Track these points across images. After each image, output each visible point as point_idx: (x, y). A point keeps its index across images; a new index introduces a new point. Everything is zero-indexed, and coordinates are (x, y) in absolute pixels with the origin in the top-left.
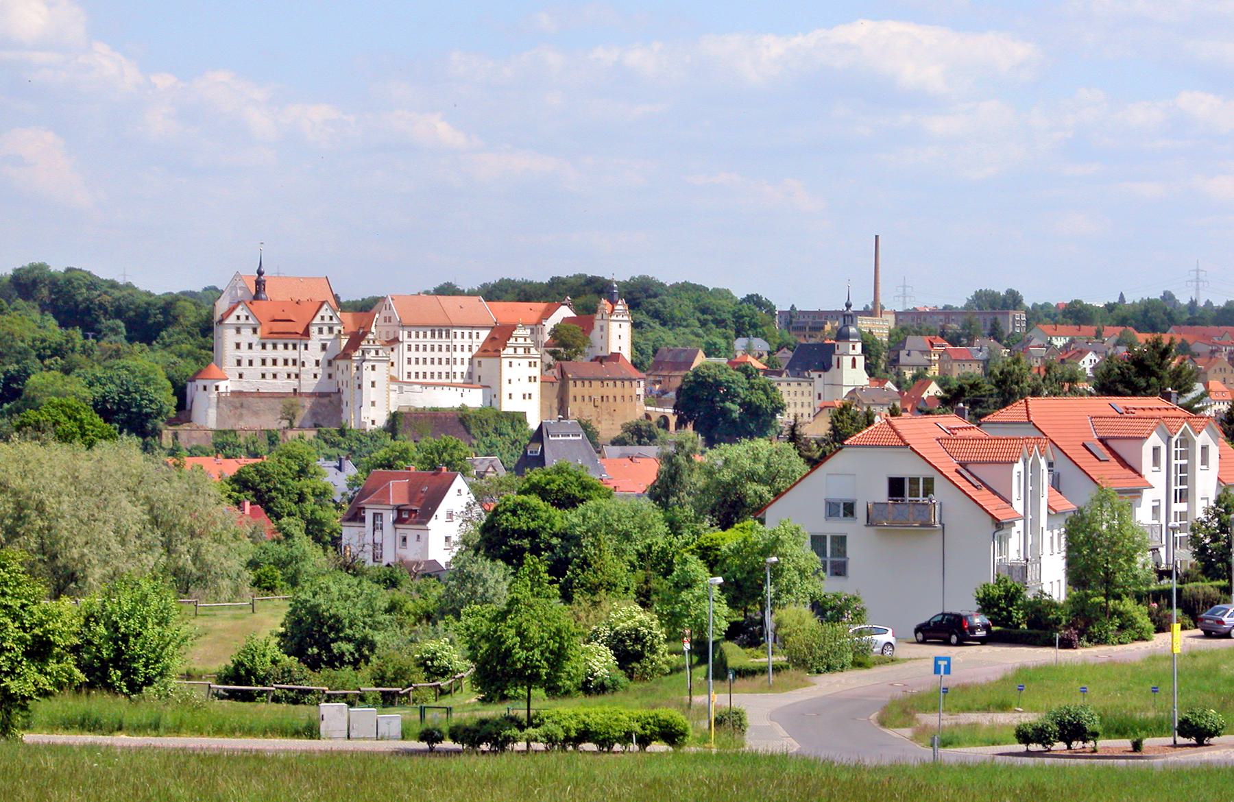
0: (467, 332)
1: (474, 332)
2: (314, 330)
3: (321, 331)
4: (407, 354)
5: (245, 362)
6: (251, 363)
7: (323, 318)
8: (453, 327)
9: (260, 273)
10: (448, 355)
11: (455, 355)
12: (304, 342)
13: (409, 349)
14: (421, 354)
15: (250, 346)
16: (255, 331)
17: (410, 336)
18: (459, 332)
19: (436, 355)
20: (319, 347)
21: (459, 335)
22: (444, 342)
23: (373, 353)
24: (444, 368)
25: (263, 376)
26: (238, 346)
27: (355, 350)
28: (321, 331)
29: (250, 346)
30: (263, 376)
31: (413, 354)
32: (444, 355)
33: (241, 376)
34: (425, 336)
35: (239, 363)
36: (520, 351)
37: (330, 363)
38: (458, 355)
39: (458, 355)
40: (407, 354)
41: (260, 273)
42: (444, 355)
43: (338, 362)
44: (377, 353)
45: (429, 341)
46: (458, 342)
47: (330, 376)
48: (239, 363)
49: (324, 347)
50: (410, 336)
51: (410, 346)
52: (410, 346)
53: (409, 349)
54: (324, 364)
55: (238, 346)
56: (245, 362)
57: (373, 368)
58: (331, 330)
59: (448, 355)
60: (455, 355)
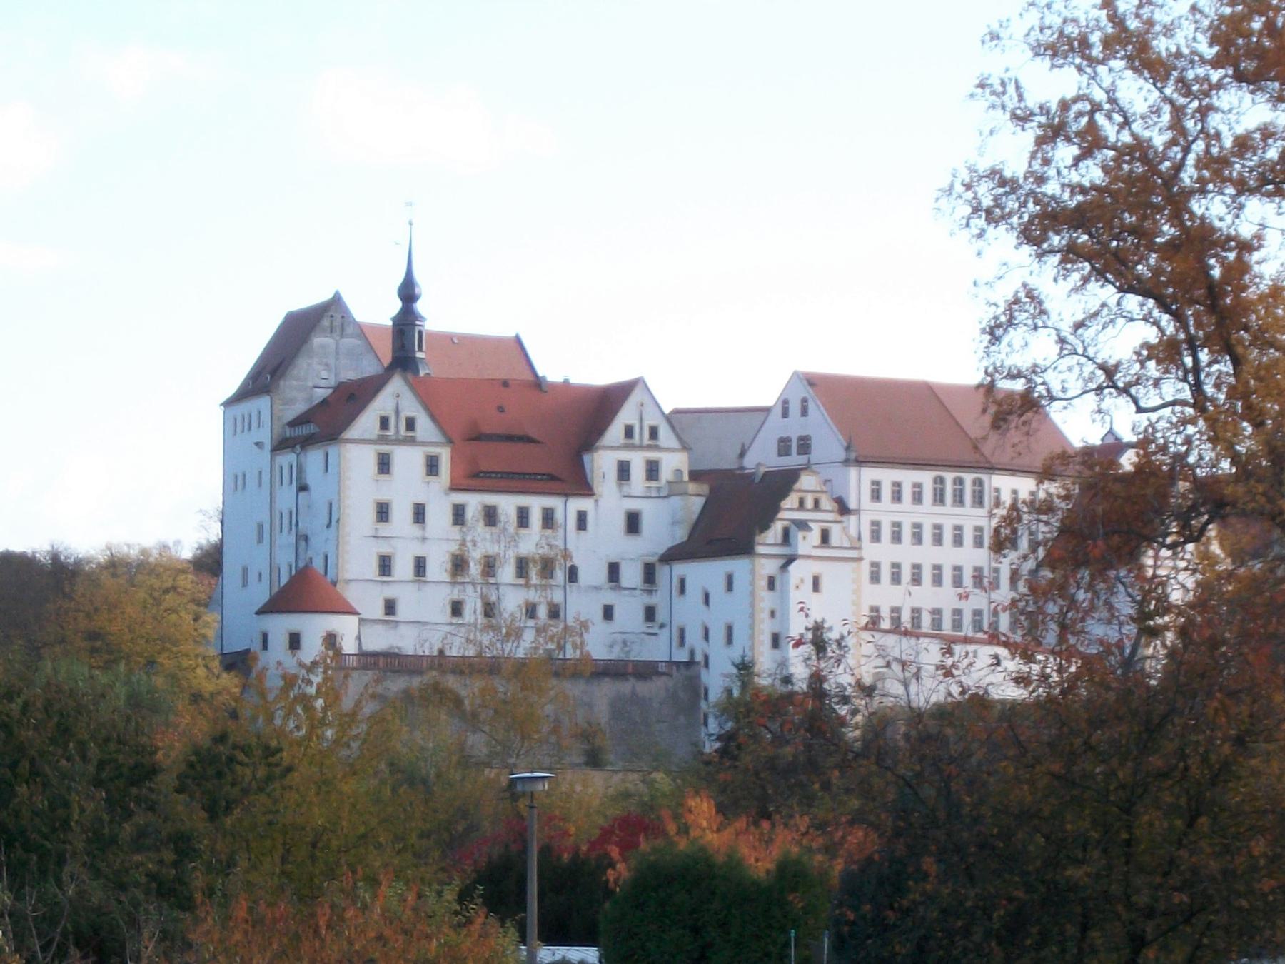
2: (602, 463)
3: (624, 471)
5: (403, 568)
6: (420, 566)
7: (629, 432)
9: (408, 293)
12: (576, 504)
14: (907, 554)
15: (419, 514)
16: (432, 466)
17: (876, 496)
20: (621, 522)
23: (815, 537)
25: (457, 609)
26: (383, 512)
27: (765, 527)
28: (624, 471)
29: (419, 514)
30: (457, 609)
31: (884, 553)
33: (390, 607)
34: (918, 498)
35: (385, 565)
37: (649, 574)
41: (408, 293)
43: (680, 569)
44: (825, 537)
45: (928, 514)
47: (650, 614)
48: (385, 565)
49: (633, 523)
50: (876, 496)
54: (631, 575)
55: (383, 512)
56: (403, 568)
57: (816, 585)
58: (653, 470)
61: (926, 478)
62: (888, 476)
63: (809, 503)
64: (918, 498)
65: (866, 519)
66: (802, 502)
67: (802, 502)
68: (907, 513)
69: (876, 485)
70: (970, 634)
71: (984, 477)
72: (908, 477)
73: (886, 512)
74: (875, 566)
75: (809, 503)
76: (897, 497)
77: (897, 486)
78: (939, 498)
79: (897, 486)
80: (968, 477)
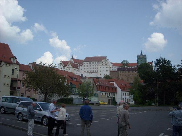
0: (97, 62)
1: (99, 62)
4: (84, 67)
8: (93, 61)
10: (92, 67)
14: (87, 67)
17: (85, 64)
18: (95, 62)
19: (90, 67)
22: (91, 64)
24: (91, 70)
31: (85, 67)
32: (91, 67)
34: (88, 64)
36: (104, 65)
38: (95, 67)
39: (95, 67)
40: (84, 67)
42: (91, 67)
50: (85, 64)
61: (88, 62)
62: (85, 63)
64: (88, 64)
72: (87, 62)
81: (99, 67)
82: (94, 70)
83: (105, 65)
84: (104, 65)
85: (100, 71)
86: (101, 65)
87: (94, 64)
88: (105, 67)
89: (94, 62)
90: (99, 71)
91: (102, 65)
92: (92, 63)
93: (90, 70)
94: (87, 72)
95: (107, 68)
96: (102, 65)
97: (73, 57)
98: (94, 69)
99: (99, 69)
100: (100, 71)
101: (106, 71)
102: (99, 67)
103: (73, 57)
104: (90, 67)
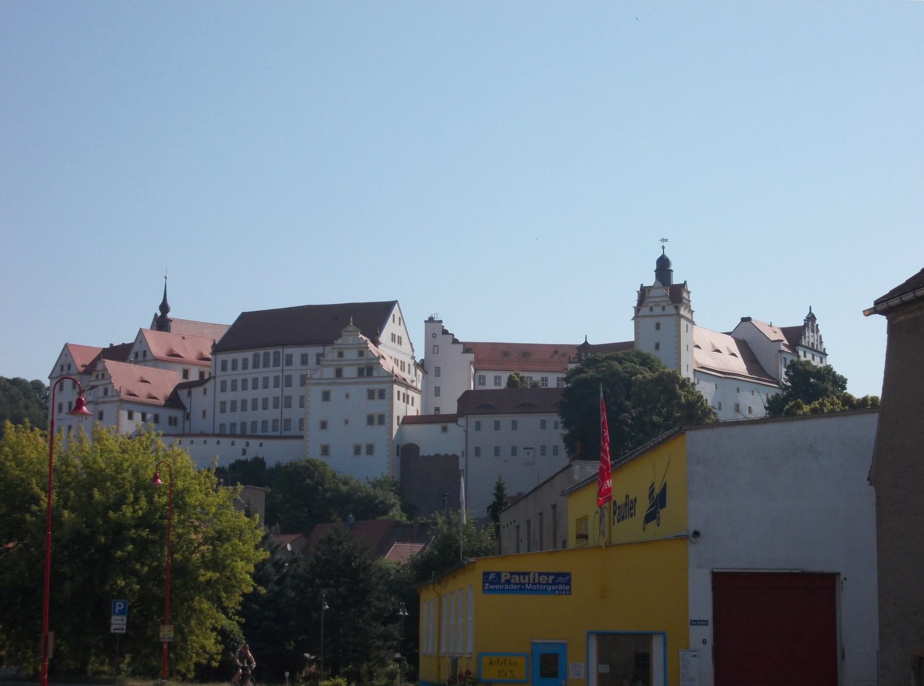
4: (221, 397)
8: (284, 345)
10: (277, 392)
11: (288, 391)
13: (223, 390)
17: (224, 369)
18: (296, 352)
19: (260, 393)
21: (296, 359)
22: (272, 372)
24: (272, 414)
31: (229, 396)
32: (272, 392)
34: (245, 367)
36: (350, 372)
38: (295, 391)
39: (295, 391)
42: (272, 392)
45: (250, 374)
46: (295, 371)
50: (224, 369)
51: (224, 383)
52: (224, 383)
53: (223, 390)
59: (277, 392)
60: (288, 391)
61: (249, 355)
63: (100, 377)
65: (219, 380)
66: (97, 376)
67: (97, 376)
68: (240, 374)
69: (224, 363)
70: (285, 433)
71: (281, 350)
72: (239, 356)
73: (229, 375)
74: (223, 404)
75: (100, 377)
76: (234, 368)
77: (235, 362)
78: (256, 366)
79: (235, 362)
80: (271, 351)
81: (315, 394)
82: (287, 413)
83: (361, 373)
84: (350, 372)
85: (324, 425)
86: (330, 373)
87: (288, 370)
88: (364, 389)
89: (288, 351)
90: (313, 424)
91: (339, 373)
92: (276, 364)
93: (259, 415)
94: (233, 435)
95: (371, 394)
96: (339, 373)
97: (164, 307)
98: (288, 406)
99: (316, 410)
100: (324, 425)
101: (370, 420)
102: (315, 394)
103: (164, 307)
104: (260, 393)
